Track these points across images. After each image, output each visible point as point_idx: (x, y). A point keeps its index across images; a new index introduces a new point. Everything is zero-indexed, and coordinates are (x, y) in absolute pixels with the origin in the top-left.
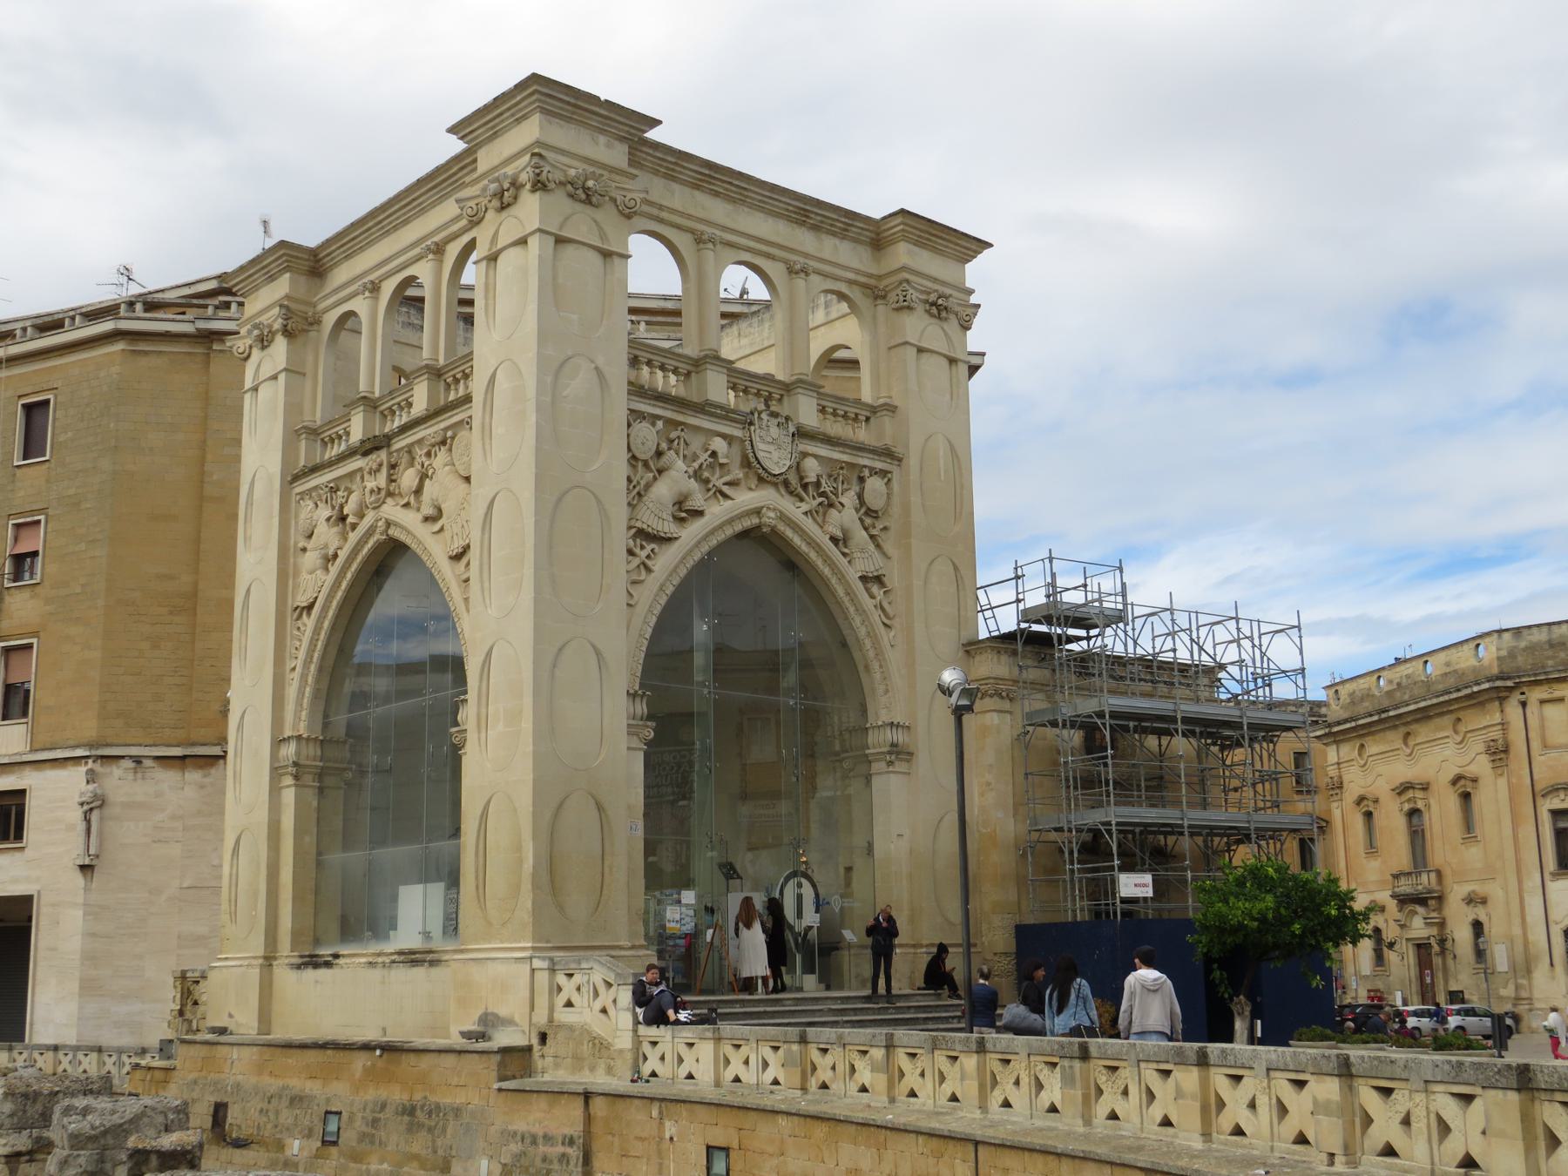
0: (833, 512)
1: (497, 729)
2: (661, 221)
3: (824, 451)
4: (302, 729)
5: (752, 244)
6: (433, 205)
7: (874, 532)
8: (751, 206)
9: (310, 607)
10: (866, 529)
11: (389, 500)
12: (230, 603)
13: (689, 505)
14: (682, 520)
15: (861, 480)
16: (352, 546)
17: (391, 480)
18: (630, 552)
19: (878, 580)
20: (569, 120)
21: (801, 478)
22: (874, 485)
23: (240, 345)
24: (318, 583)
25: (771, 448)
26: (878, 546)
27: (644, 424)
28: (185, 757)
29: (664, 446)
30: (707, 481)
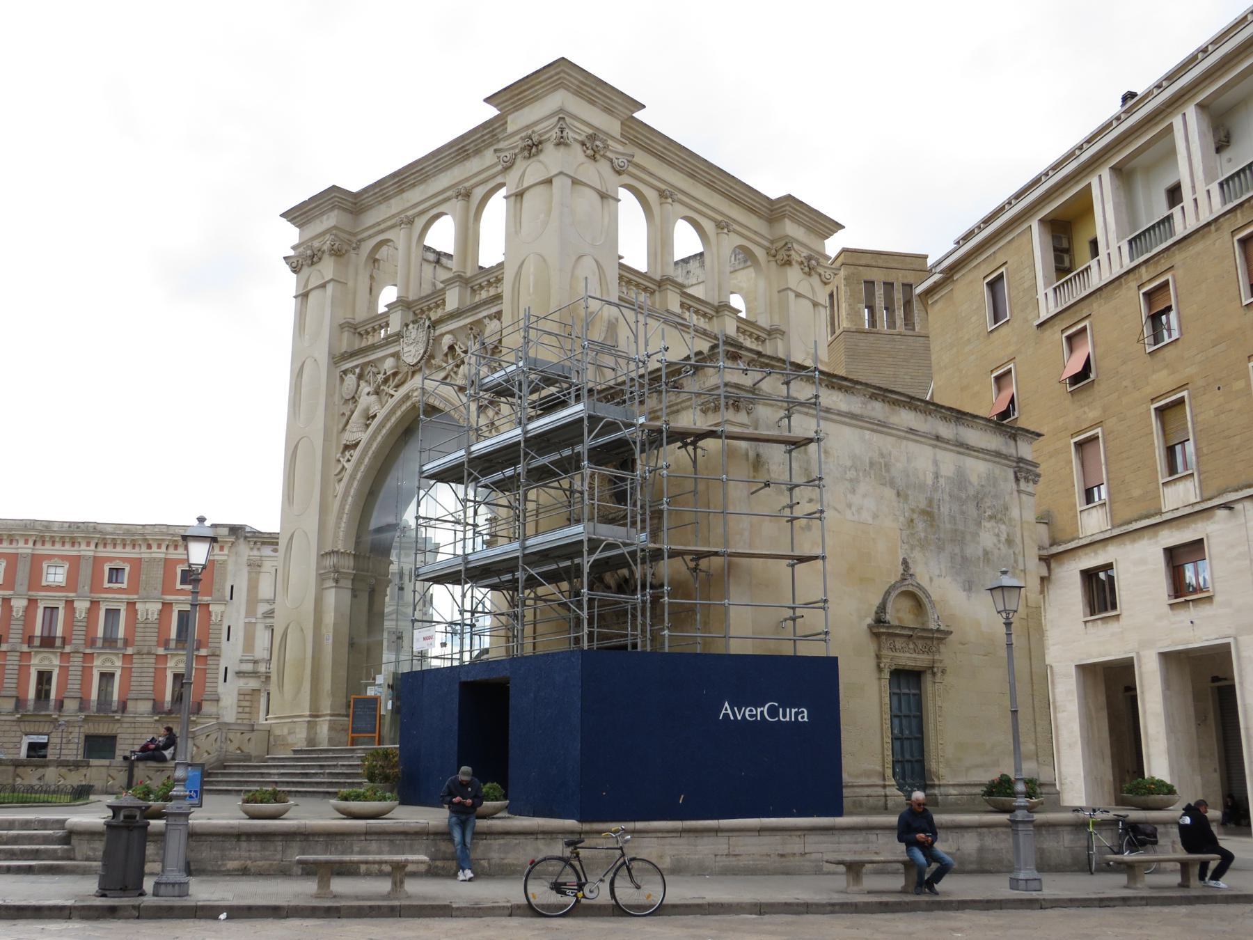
5: (433, 201)
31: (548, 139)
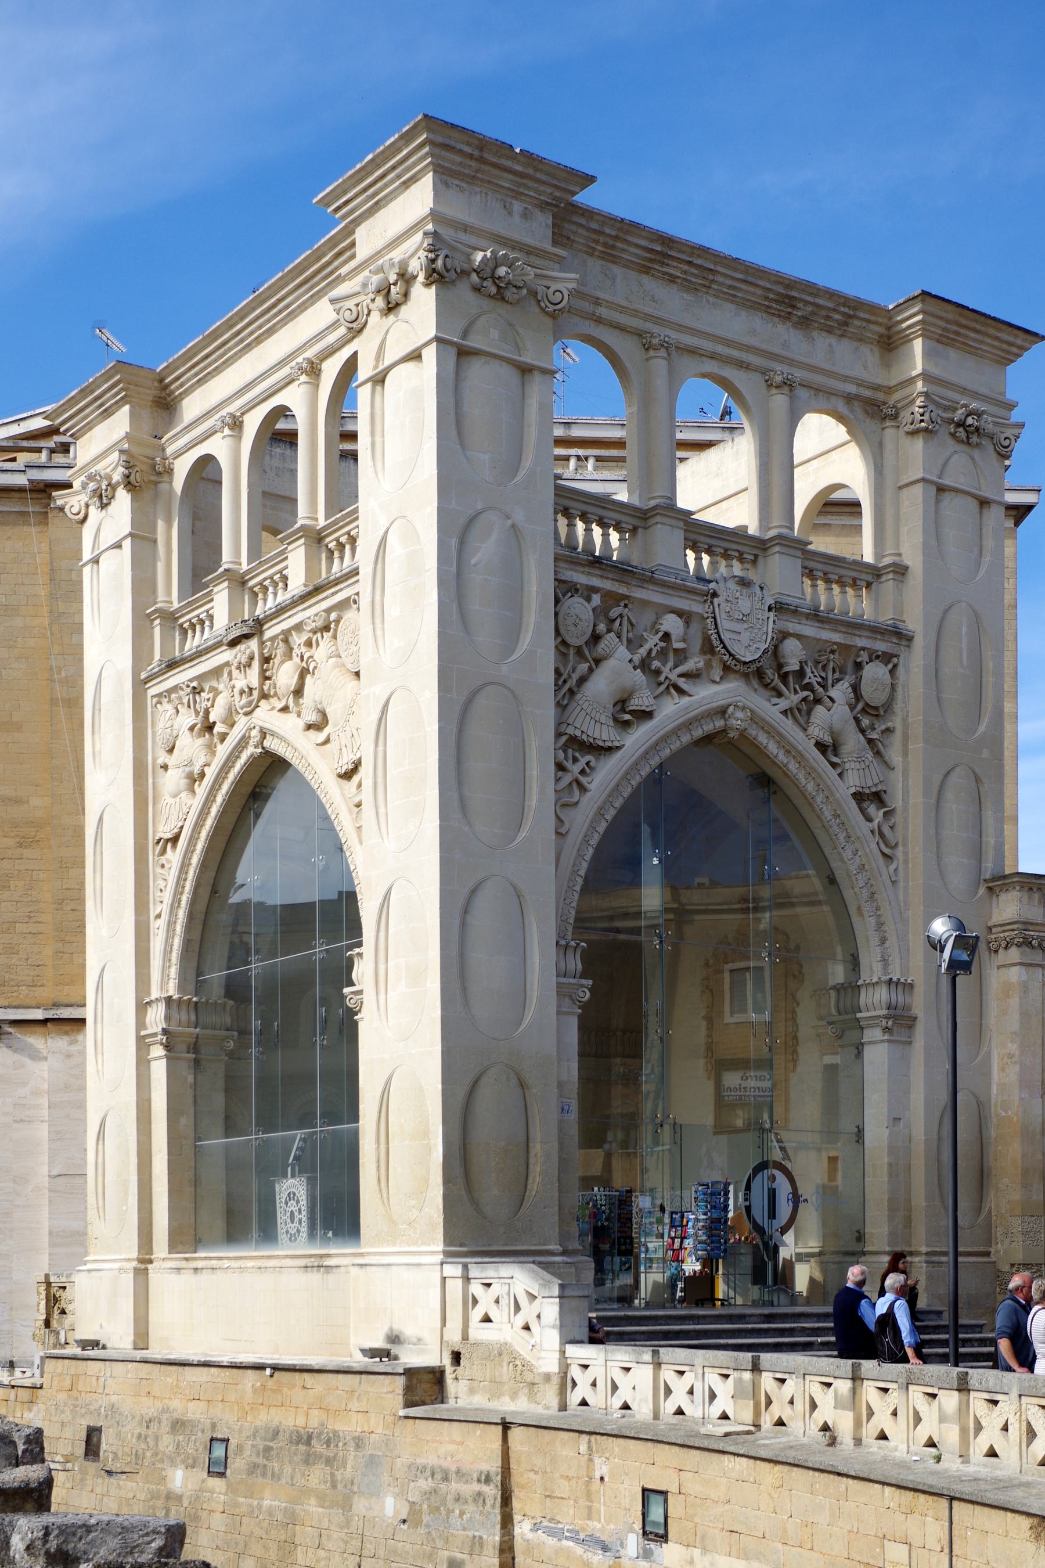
0: (819, 709)
1: (398, 990)
3: (809, 630)
4: (172, 991)
6: (303, 307)
7: (874, 736)
9: (175, 840)
10: (863, 731)
11: (263, 703)
12: (79, 833)
13: (634, 704)
14: (626, 724)
15: (858, 666)
16: (220, 763)
17: (265, 677)
18: (560, 767)
19: (878, 798)
20: (472, 179)
21: (780, 666)
22: (874, 672)
23: (73, 502)
24: (185, 809)
26: (878, 753)
27: (577, 600)
28: (45, 1021)
29: (602, 627)
30: (658, 672)
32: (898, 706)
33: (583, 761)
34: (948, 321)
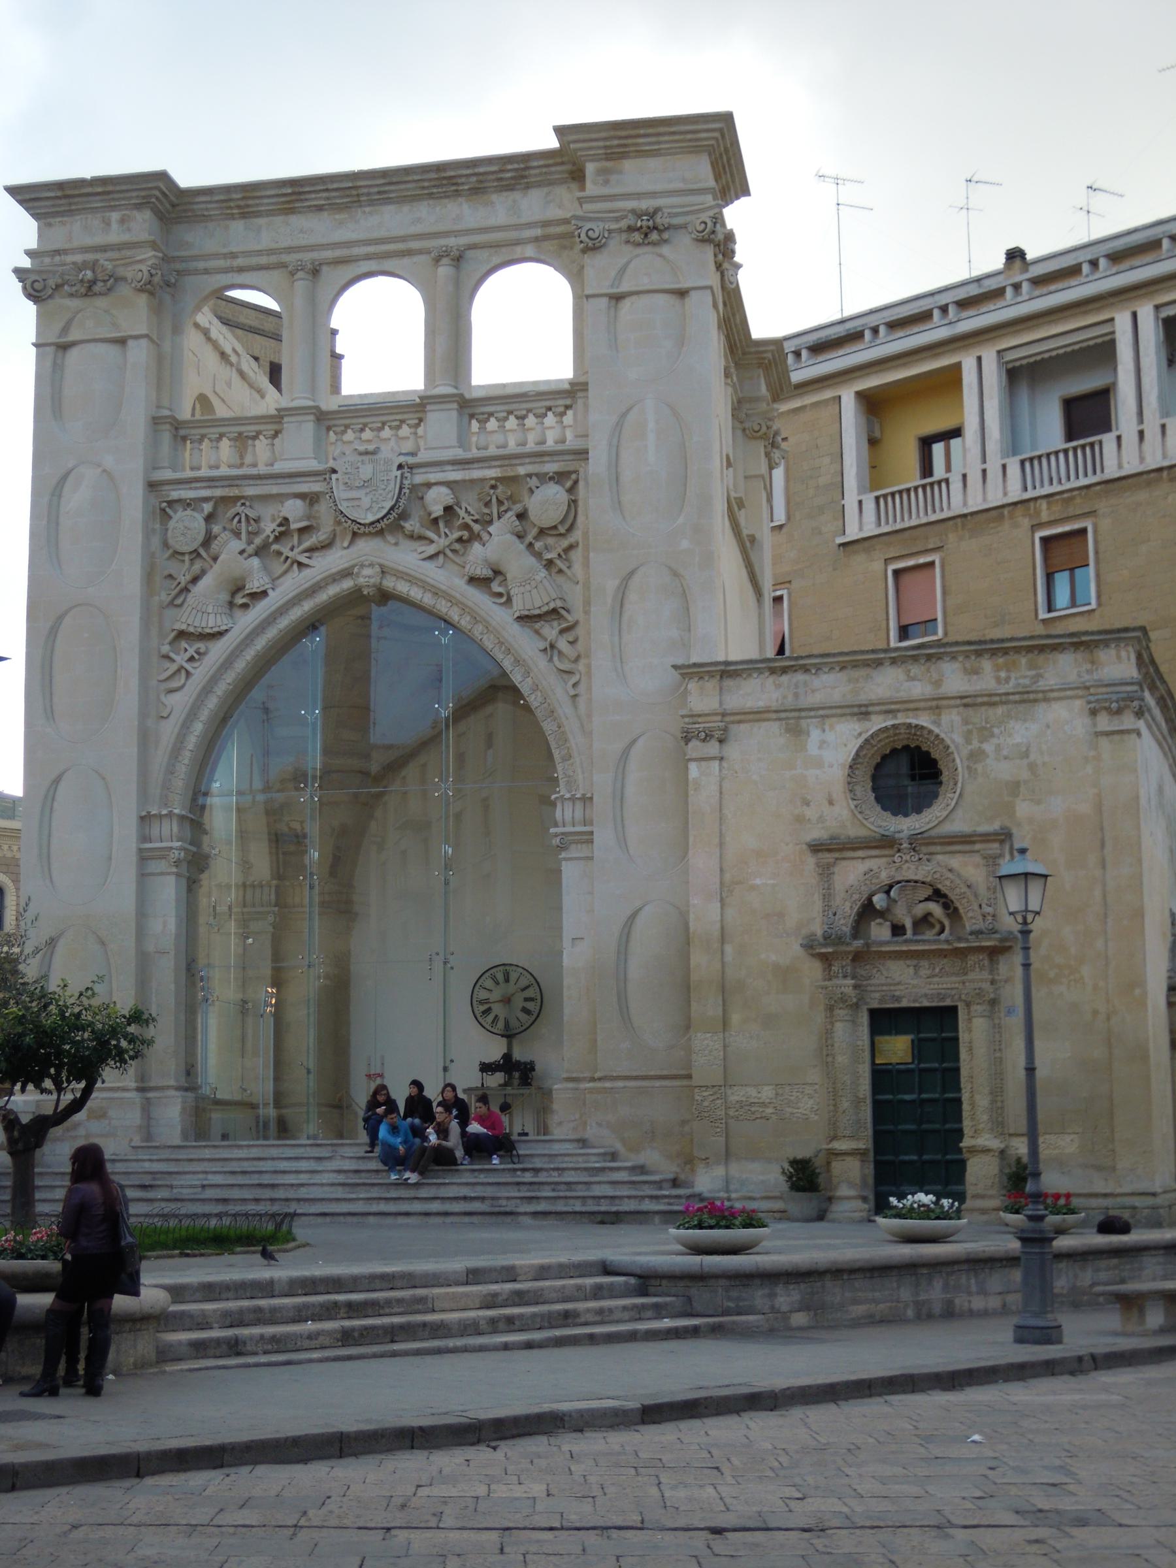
0: (476, 547)
2: (241, 270)
5: (371, 249)
8: (372, 203)
10: (538, 555)
25: (360, 494)
27: (189, 512)
31: (684, 227)
32: (581, 519)
33: (191, 651)
34: (605, 139)
